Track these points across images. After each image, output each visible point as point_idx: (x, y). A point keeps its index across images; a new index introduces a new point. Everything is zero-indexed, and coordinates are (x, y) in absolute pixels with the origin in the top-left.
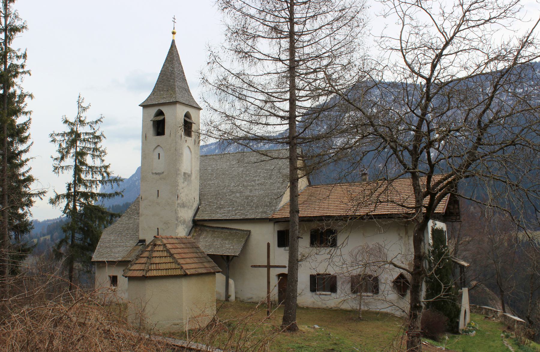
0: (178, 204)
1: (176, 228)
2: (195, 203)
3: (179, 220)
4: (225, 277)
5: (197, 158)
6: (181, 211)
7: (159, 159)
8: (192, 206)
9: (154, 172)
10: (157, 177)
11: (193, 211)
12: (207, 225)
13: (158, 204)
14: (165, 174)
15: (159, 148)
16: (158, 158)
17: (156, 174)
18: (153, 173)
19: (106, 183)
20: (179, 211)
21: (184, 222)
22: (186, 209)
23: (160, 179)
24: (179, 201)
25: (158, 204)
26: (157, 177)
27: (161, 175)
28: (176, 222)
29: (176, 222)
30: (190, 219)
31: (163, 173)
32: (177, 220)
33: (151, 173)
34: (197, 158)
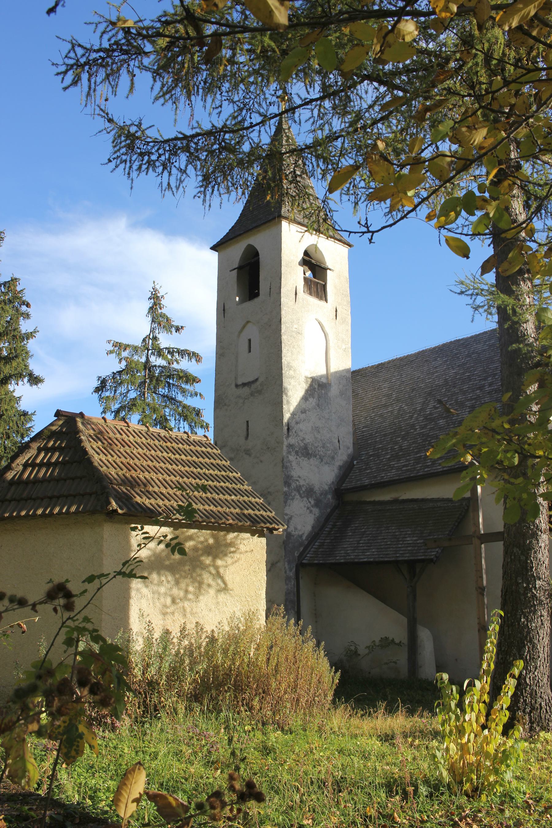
0: (290, 446)
1: (285, 502)
2: (340, 452)
3: (293, 485)
4: (405, 620)
5: (345, 350)
6: (298, 464)
7: (250, 351)
8: (333, 458)
9: (240, 383)
10: (246, 390)
11: (336, 471)
12: (368, 500)
13: (248, 452)
14: (260, 380)
15: (250, 325)
16: (247, 350)
17: (244, 385)
18: (237, 386)
19: (506, 772)
20: (294, 464)
21: (309, 492)
22: (313, 461)
23: (252, 394)
24: (292, 440)
25: (248, 452)
26: (246, 391)
27: (254, 386)
28: (286, 489)
29: (286, 489)
30: (326, 488)
31: (257, 380)
32: (287, 483)
33: (233, 386)
34: (345, 350)
